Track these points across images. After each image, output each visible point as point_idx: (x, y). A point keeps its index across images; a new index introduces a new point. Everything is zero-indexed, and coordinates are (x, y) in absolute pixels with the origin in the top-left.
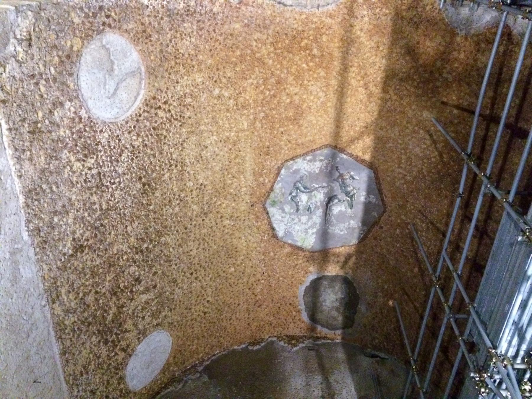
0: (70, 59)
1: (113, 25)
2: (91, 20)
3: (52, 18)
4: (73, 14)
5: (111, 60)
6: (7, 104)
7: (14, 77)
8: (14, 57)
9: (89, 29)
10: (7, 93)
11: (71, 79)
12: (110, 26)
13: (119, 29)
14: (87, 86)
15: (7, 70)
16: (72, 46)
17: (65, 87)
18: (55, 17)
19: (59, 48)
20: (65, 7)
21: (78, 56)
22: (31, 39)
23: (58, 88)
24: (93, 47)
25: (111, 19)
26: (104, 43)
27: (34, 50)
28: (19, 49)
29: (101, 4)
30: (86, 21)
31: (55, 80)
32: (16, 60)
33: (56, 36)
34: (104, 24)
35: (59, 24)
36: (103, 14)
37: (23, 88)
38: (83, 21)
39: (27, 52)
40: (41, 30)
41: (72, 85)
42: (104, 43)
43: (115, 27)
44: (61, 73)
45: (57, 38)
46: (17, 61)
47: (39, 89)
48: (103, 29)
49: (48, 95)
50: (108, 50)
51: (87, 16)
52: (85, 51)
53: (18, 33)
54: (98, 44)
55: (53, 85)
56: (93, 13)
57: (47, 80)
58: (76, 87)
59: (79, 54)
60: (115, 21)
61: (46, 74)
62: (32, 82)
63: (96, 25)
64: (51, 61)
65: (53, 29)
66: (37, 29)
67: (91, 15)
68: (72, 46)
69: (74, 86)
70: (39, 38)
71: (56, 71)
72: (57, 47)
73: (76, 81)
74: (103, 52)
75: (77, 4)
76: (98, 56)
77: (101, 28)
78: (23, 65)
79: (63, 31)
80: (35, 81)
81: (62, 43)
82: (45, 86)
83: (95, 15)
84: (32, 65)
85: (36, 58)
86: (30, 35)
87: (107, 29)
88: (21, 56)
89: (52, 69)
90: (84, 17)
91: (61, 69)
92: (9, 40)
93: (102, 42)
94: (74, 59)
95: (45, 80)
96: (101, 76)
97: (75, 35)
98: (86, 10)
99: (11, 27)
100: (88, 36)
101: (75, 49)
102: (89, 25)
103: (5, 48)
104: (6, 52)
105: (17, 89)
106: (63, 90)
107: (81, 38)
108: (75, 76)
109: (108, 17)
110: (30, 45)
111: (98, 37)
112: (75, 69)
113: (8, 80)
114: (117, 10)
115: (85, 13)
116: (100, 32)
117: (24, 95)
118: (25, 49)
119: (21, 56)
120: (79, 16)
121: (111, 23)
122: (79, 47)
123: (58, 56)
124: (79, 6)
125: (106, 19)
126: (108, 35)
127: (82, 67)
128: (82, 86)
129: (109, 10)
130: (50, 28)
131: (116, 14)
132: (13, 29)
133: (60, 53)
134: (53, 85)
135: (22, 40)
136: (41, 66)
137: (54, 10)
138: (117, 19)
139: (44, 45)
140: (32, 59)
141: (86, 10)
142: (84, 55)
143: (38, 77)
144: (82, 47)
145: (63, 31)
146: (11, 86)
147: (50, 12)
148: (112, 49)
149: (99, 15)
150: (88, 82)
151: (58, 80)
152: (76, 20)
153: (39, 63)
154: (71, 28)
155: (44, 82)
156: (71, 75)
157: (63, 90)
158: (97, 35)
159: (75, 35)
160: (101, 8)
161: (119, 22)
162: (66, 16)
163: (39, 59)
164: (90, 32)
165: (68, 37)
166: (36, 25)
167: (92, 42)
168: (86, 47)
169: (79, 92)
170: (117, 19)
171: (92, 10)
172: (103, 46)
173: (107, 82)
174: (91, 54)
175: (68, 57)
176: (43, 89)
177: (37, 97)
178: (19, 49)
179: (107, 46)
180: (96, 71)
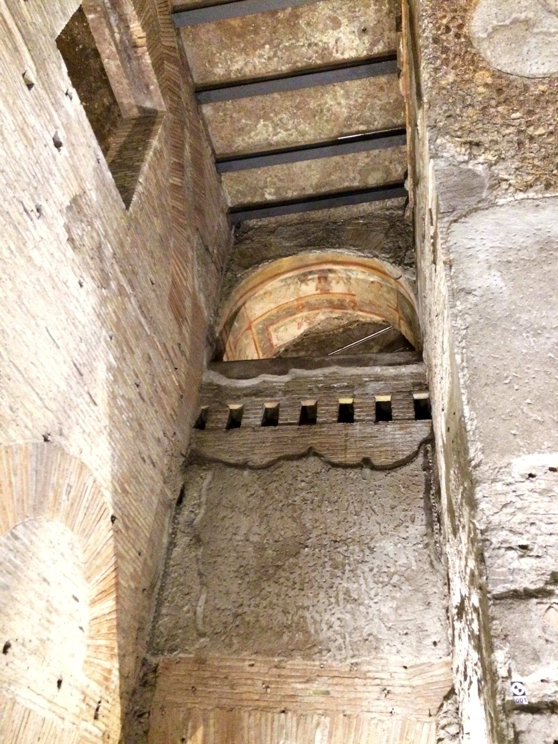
0: (504, 88)
1: (460, 21)
2: (451, 56)
3: (445, 111)
4: (443, 82)
5: (511, 23)
6: (552, 182)
7: (517, 169)
8: (491, 166)
9: (463, 60)
10: (537, 180)
11: (532, 89)
12: (461, 26)
13: (465, 10)
14: (547, 64)
15: (506, 177)
16: (486, 85)
17: (542, 98)
18: (445, 107)
19: (486, 105)
20: (434, 93)
21: (500, 77)
22: (470, 143)
23: (543, 108)
24: (489, 53)
25: (451, 25)
26: (485, 35)
27: (485, 139)
28: (481, 159)
29: (430, 40)
30: (451, 65)
31: (530, 112)
32: (495, 164)
33: (470, 108)
34: (457, 36)
35: (454, 103)
36: (444, 37)
37: (533, 158)
38: (453, 68)
39: (486, 149)
40: (461, 128)
41: (542, 88)
42: (485, 35)
43: (463, 18)
44: (521, 104)
45: (473, 106)
46: (496, 163)
47: (540, 135)
48: (465, 37)
49: (551, 124)
50: (495, 29)
51: (446, 62)
52: (494, 66)
53: (461, 158)
54: (485, 45)
55: (538, 116)
56: (442, 53)
57: (529, 124)
58: (546, 81)
59: (498, 75)
60: (454, 18)
61: (520, 124)
62: (527, 146)
63: (458, 48)
64: (503, 117)
65: (461, 111)
66: (459, 133)
67: (444, 56)
68: (486, 85)
69: (544, 84)
70: (470, 132)
71: (517, 111)
72: (486, 107)
73: (536, 81)
74: (497, 37)
75: (431, 76)
76: (503, 45)
77: (463, 40)
78: (503, 156)
79: (463, 97)
80: (527, 141)
81: (480, 99)
82: (536, 129)
83: (445, 50)
84: (505, 144)
85: (496, 136)
86: (465, 143)
87: (465, 30)
88: (490, 157)
89: (514, 116)
90: (447, 66)
91: (515, 102)
92: (470, 170)
93: (483, 39)
94: (504, 82)
95: (528, 127)
96: (533, 41)
97: (470, 81)
98: (439, 62)
99: (454, 165)
100: (473, 61)
101: (489, 80)
102: (458, 59)
103: (478, 176)
104: (483, 175)
105: (534, 166)
106: (548, 102)
107: (475, 71)
108: (528, 82)
109: (448, 29)
110: (478, 144)
111: (475, 45)
112: (519, 82)
113: (519, 178)
114: (439, 14)
115: (442, 64)
116: (469, 43)
117: (544, 158)
118: (482, 151)
119: (490, 157)
120: (446, 73)
121: (456, 24)
122: (487, 74)
123: (497, 106)
124: (433, 73)
125: (452, 33)
126: (474, 29)
127: (518, 71)
128: (546, 71)
129: (439, 29)
130: (459, 116)
131: (445, 17)
132: (456, 163)
133: (493, 103)
134: (538, 116)
135: (470, 154)
136: (507, 131)
137: (437, 109)
138: (452, 14)
139: (480, 125)
140: (496, 142)
141: (439, 62)
142: (499, 68)
143: (522, 137)
144: (488, 70)
145: (463, 97)
146: (528, 174)
147: (439, 114)
148: (495, 23)
149: (445, 44)
150: (540, 63)
151: (531, 108)
152: (451, 77)
153: (504, 133)
154: (461, 86)
155: (531, 128)
156: (526, 88)
157: (548, 102)
158: (473, 47)
159: (470, 81)
160: (436, 40)
161: (455, 11)
162: (444, 92)
163: (498, 132)
164: (468, 57)
165: (473, 90)
166: (453, 134)
167: (483, 55)
168: (489, 63)
169: (554, 76)
170: (452, 14)
171: (439, 53)
172: (490, 36)
173: (544, 30)
174: (501, 57)
175: (500, 91)
176: (541, 131)
177: (550, 140)
178: (481, 159)
179: (490, 30)
180: (525, 49)
